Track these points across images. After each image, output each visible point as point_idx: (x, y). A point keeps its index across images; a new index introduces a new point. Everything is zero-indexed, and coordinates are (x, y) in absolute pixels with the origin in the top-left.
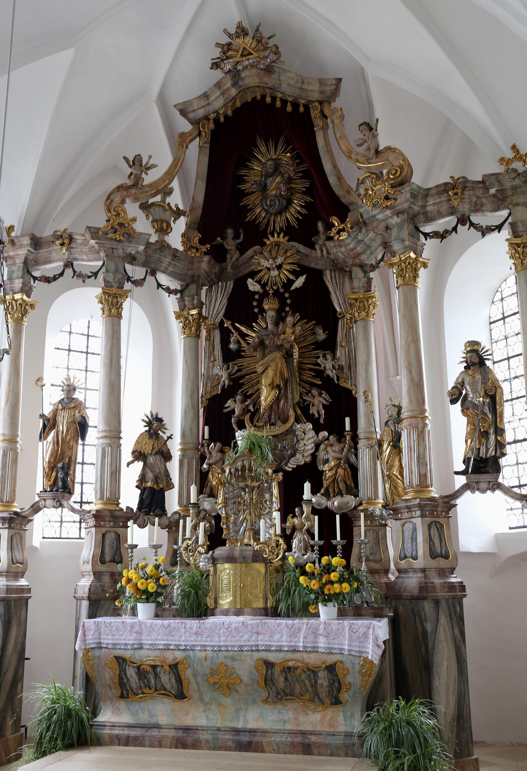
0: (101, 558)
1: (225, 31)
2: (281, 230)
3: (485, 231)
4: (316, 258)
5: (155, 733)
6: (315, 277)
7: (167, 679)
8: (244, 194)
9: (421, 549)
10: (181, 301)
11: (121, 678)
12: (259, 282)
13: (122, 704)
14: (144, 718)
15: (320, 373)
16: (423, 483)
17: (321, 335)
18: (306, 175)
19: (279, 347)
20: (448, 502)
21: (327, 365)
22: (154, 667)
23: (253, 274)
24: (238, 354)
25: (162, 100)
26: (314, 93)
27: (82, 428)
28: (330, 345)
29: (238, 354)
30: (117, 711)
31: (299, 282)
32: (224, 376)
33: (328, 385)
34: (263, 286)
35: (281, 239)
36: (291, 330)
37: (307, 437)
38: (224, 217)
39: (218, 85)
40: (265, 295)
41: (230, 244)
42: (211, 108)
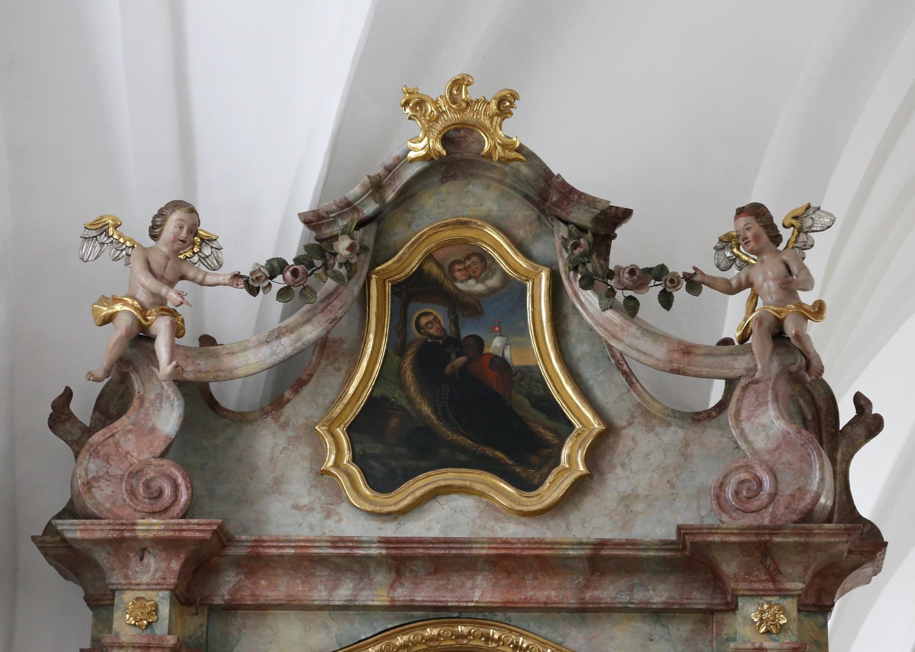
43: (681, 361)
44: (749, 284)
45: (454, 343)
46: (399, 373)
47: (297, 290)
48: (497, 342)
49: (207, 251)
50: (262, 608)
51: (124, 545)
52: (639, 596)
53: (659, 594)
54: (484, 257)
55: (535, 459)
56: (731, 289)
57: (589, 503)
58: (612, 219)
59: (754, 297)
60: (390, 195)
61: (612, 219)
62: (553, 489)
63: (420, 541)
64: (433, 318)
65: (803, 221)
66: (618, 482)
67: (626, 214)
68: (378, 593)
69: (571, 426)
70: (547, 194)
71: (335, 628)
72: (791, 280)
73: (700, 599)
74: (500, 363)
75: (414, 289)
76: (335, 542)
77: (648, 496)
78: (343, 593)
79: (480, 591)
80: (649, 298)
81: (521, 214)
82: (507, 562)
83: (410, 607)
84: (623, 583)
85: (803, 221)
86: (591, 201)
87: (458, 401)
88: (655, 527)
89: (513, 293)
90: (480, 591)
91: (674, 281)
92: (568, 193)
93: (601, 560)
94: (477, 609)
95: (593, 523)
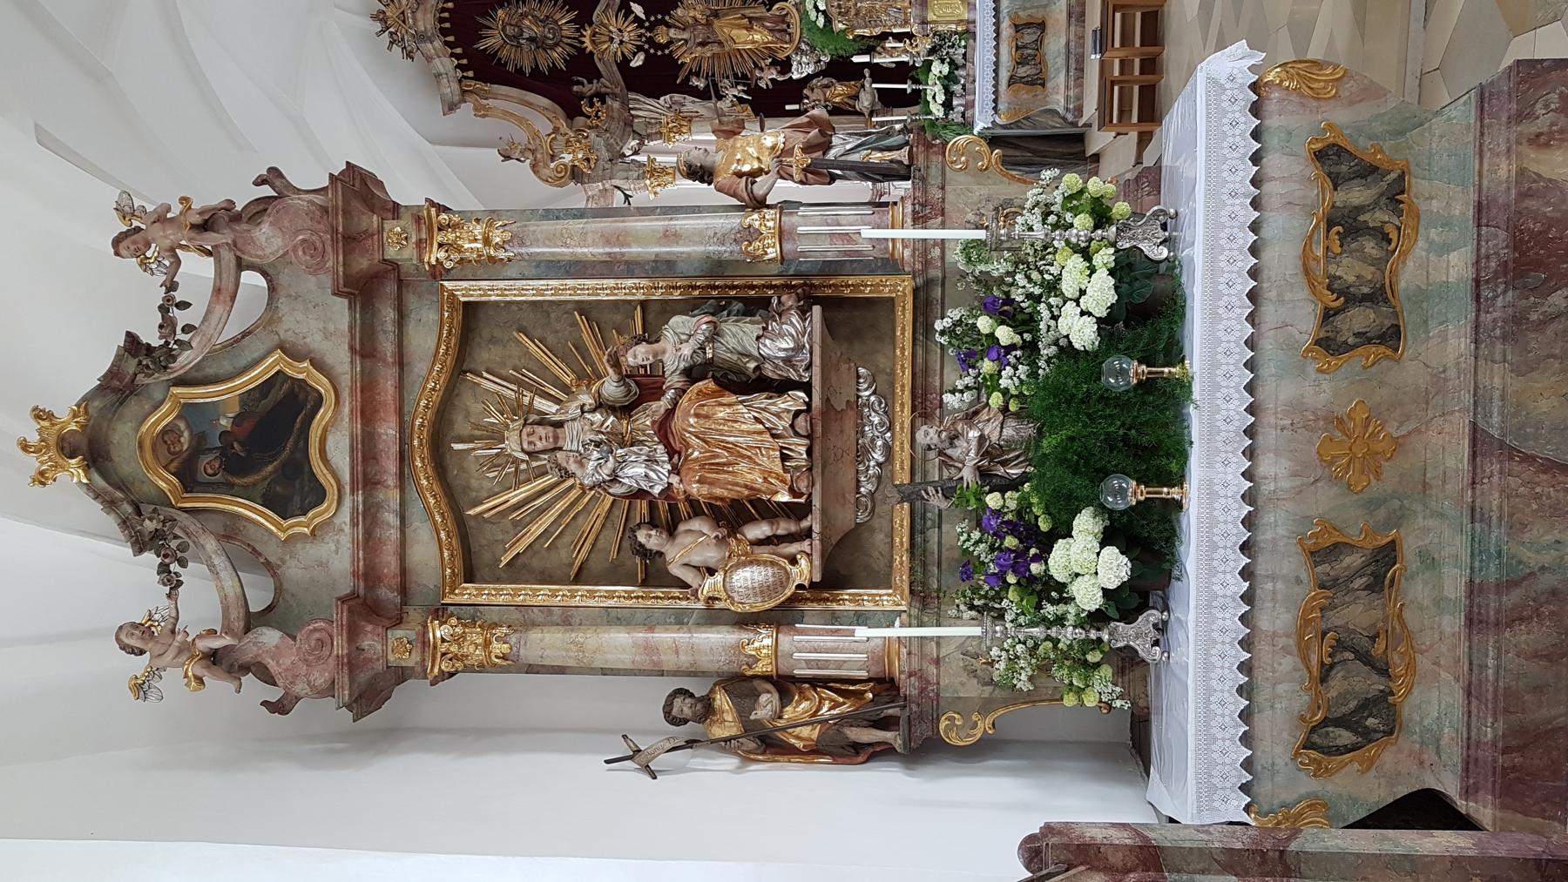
1: (378, 34)
2: (578, 30)
5: (1072, 44)
7: (1029, 37)
8: (536, 70)
10: (650, 137)
11: (1027, 83)
12: (634, 54)
13: (1049, 85)
14: (1061, 61)
19: (709, 24)
22: (1018, 48)
30: (1056, 90)
31: (638, 9)
32: (732, 92)
34: (640, 48)
35: (588, 33)
39: (429, 59)
40: (650, 41)
41: (589, 88)
42: (452, 73)
43: (226, 295)
44: (172, 250)
45: (225, 451)
46: (245, 487)
47: (179, 554)
48: (223, 422)
49: (156, 617)
50: (403, 571)
51: (353, 663)
52: (390, 327)
53: (388, 314)
54: (165, 431)
55: (301, 396)
56: (178, 262)
57: (330, 360)
58: (133, 344)
59: (182, 247)
60: (119, 494)
61: (133, 344)
62: (321, 384)
63: (352, 468)
64: (207, 465)
66: (316, 341)
67: (129, 334)
68: (390, 496)
69: (278, 372)
70: (117, 388)
71: (416, 524)
73: (391, 288)
74: (237, 420)
75: (189, 480)
76: (354, 524)
78: (392, 519)
79: (388, 431)
80: (182, 317)
81: (133, 407)
82: (368, 413)
83: (401, 476)
84: (381, 337)
86: (119, 358)
87: (263, 446)
89: (189, 411)
90: (388, 431)
91: (168, 299)
92: (113, 373)
93: (365, 349)
94: (401, 430)
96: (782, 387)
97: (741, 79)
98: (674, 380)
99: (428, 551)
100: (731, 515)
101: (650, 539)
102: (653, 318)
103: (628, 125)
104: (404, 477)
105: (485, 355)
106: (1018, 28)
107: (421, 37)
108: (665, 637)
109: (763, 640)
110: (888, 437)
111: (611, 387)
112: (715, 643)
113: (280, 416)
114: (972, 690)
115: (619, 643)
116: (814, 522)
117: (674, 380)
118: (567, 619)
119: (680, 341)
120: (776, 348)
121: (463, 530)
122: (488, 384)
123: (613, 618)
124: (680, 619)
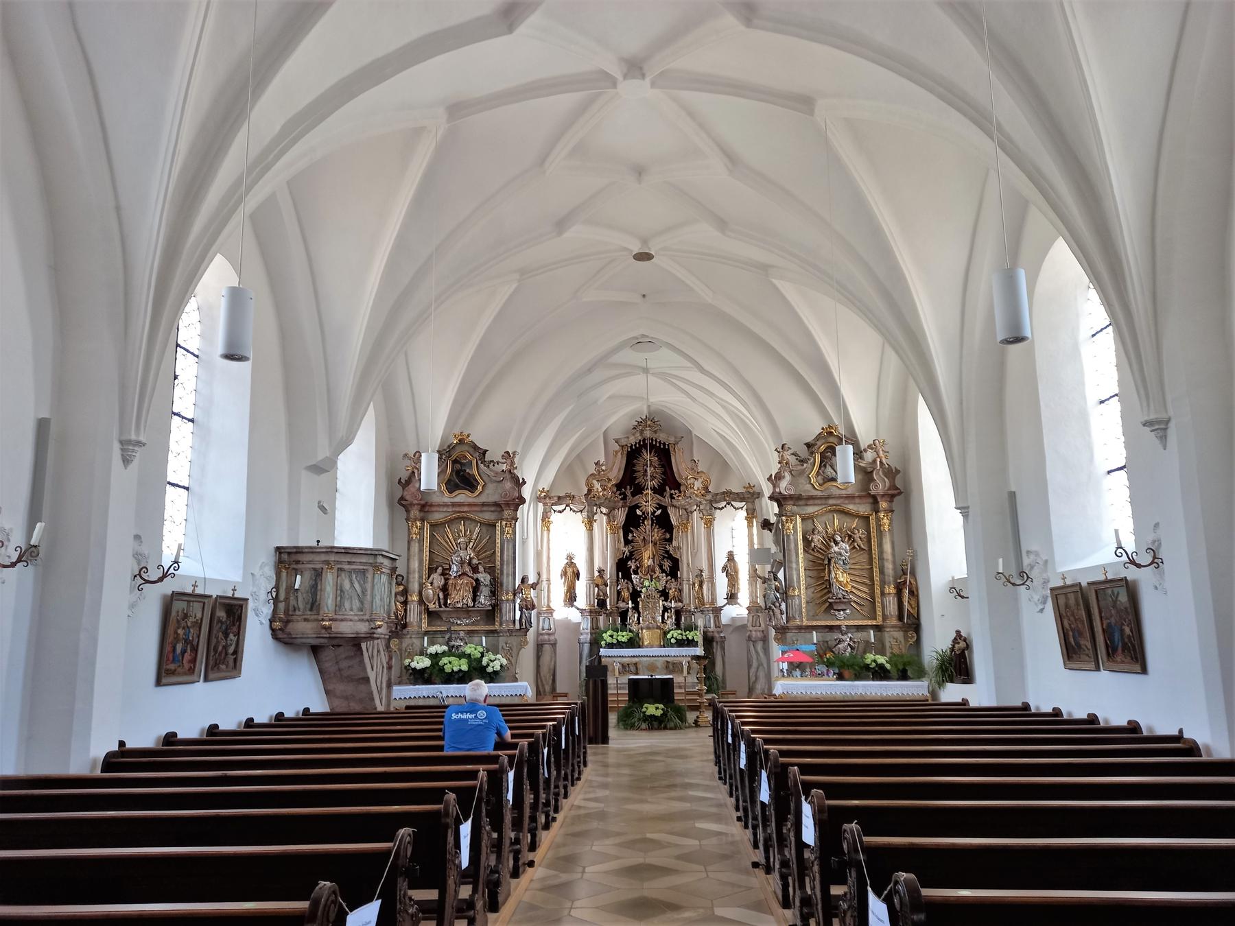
0: (592, 628)
3: (736, 509)
4: (666, 501)
6: (664, 509)
8: (635, 471)
9: (712, 625)
15: (667, 552)
16: (714, 600)
17: (668, 536)
18: (663, 466)
20: (720, 609)
21: (670, 548)
23: (637, 506)
24: (632, 541)
25: (605, 434)
26: (672, 440)
27: (577, 575)
28: (670, 540)
29: (632, 541)
31: (659, 512)
32: (626, 550)
33: (670, 557)
36: (657, 534)
37: (663, 577)
38: (629, 483)
41: (628, 493)
51: (412, 505)
62: (477, 493)
64: (458, 466)
65: (514, 453)
66: (487, 492)
68: (450, 509)
70: (475, 447)
72: (512, 463)
75: (455, 462)
77: (490, 494)
79: (466, 509)
81: (471, 450)
82: (470, 505)
85: (514, 453)
88: (492, 499)
90: (466, 509)
93: (483, 505)
95: (483, 499)
96: (474, 600)
97: (631, 553)
98: (475, 576)
99: (437, 517)
100: (445, 589)
101: (440, 570)
102: (491, 570)
103: (612, 509)
104: (455, 512)
105: (484, 529)
106: (635, 664)
107: (642, 432)
108: (417, 575)
109: (415, 598)
110: (463, 624)
111: (475, 561)
112: (415, 586)
113: (468, 483)
114: (404, 645)
115: (415, 564)
116: (443, 608)
117: (475, 576)
118: (421, 551)
119: (484, 577)
120: (482, 599)
121: (443, 524)
122: (477, 529)
123: (421, 561)
124: (421, 577)
